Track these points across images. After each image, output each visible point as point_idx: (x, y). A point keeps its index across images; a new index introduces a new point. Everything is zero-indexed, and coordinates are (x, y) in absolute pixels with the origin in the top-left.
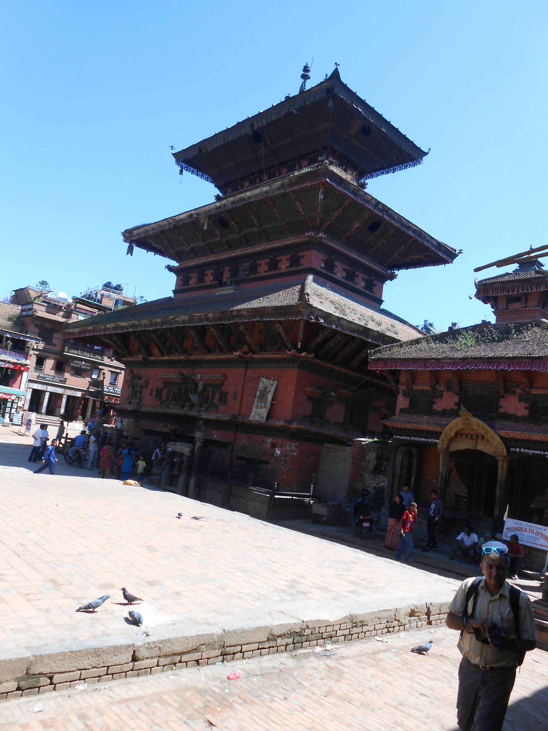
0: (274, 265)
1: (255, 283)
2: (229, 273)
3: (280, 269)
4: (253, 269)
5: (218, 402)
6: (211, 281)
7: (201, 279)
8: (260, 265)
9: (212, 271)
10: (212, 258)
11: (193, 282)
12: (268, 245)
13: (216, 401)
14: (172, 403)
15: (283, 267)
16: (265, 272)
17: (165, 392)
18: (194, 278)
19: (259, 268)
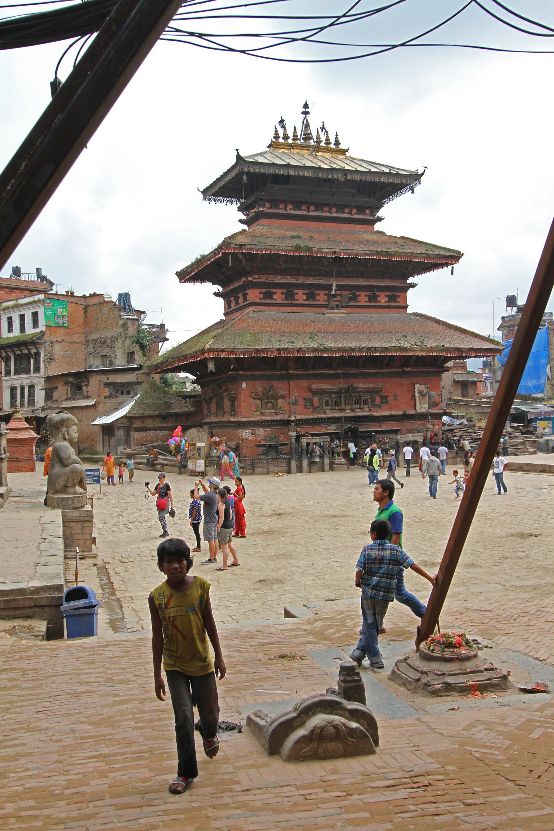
0: (373, 298)
1: (357, 309)
3: (380, 302)
4: (354, 298)
5: (380, 404)
6: (304, 300)
7: (290, 295)
8: (360, 295)
10: (302, 280)
11: (279, 296)
12: (367, 282)
14: (327, 408)
15: (383, 301)
16: (366, 302)
17: (316, 400)
19: (358, 297)
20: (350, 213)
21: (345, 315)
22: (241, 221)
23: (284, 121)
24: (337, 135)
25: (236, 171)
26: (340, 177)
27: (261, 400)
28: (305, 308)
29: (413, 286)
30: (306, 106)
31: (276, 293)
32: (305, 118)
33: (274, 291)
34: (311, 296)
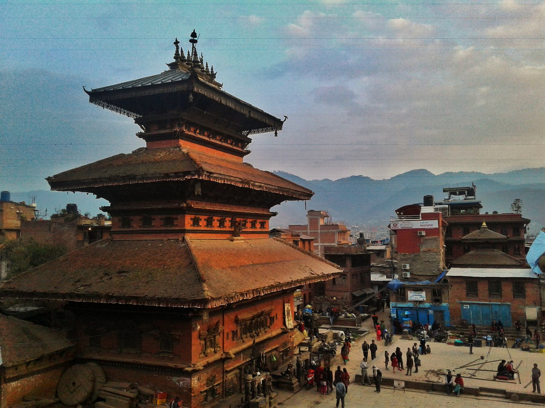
2: (230, 223)
7: (209, 223)
9: (219, 218)
13: (268, 324)
17: (238, 331)
18: (203, 220)
20: (231, 144)
21: (243, 241)
22: (140, 135)
23: (179, 42)
24: (212, 69)
25: (185, 87)
26: (245, 112)
27: (205, 340)
28: (218, 235)
29: (275, 214)
30: (194, 35)
31: (201, 219)
32: (193, 45)
33: (201, 217)
34: (222, 223)
